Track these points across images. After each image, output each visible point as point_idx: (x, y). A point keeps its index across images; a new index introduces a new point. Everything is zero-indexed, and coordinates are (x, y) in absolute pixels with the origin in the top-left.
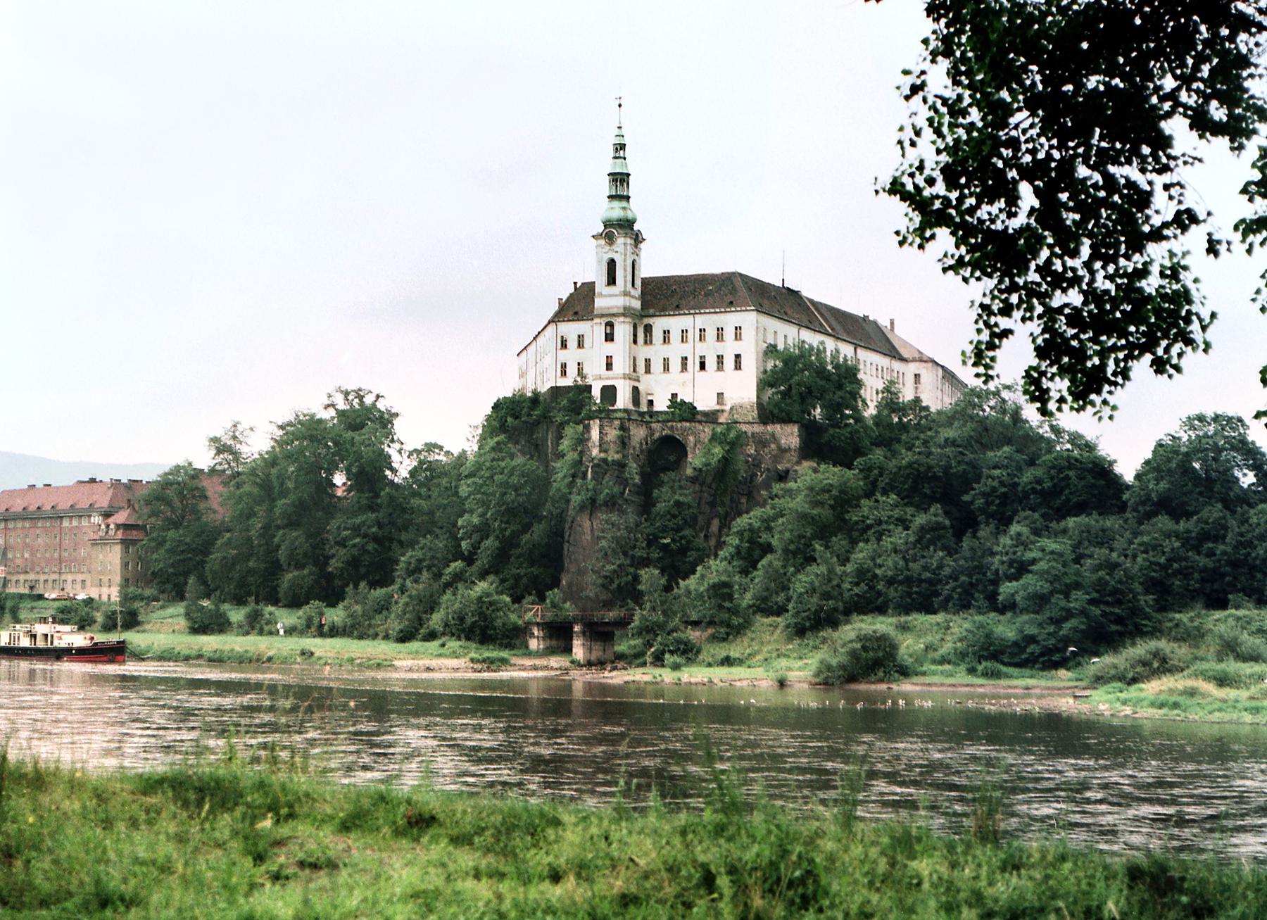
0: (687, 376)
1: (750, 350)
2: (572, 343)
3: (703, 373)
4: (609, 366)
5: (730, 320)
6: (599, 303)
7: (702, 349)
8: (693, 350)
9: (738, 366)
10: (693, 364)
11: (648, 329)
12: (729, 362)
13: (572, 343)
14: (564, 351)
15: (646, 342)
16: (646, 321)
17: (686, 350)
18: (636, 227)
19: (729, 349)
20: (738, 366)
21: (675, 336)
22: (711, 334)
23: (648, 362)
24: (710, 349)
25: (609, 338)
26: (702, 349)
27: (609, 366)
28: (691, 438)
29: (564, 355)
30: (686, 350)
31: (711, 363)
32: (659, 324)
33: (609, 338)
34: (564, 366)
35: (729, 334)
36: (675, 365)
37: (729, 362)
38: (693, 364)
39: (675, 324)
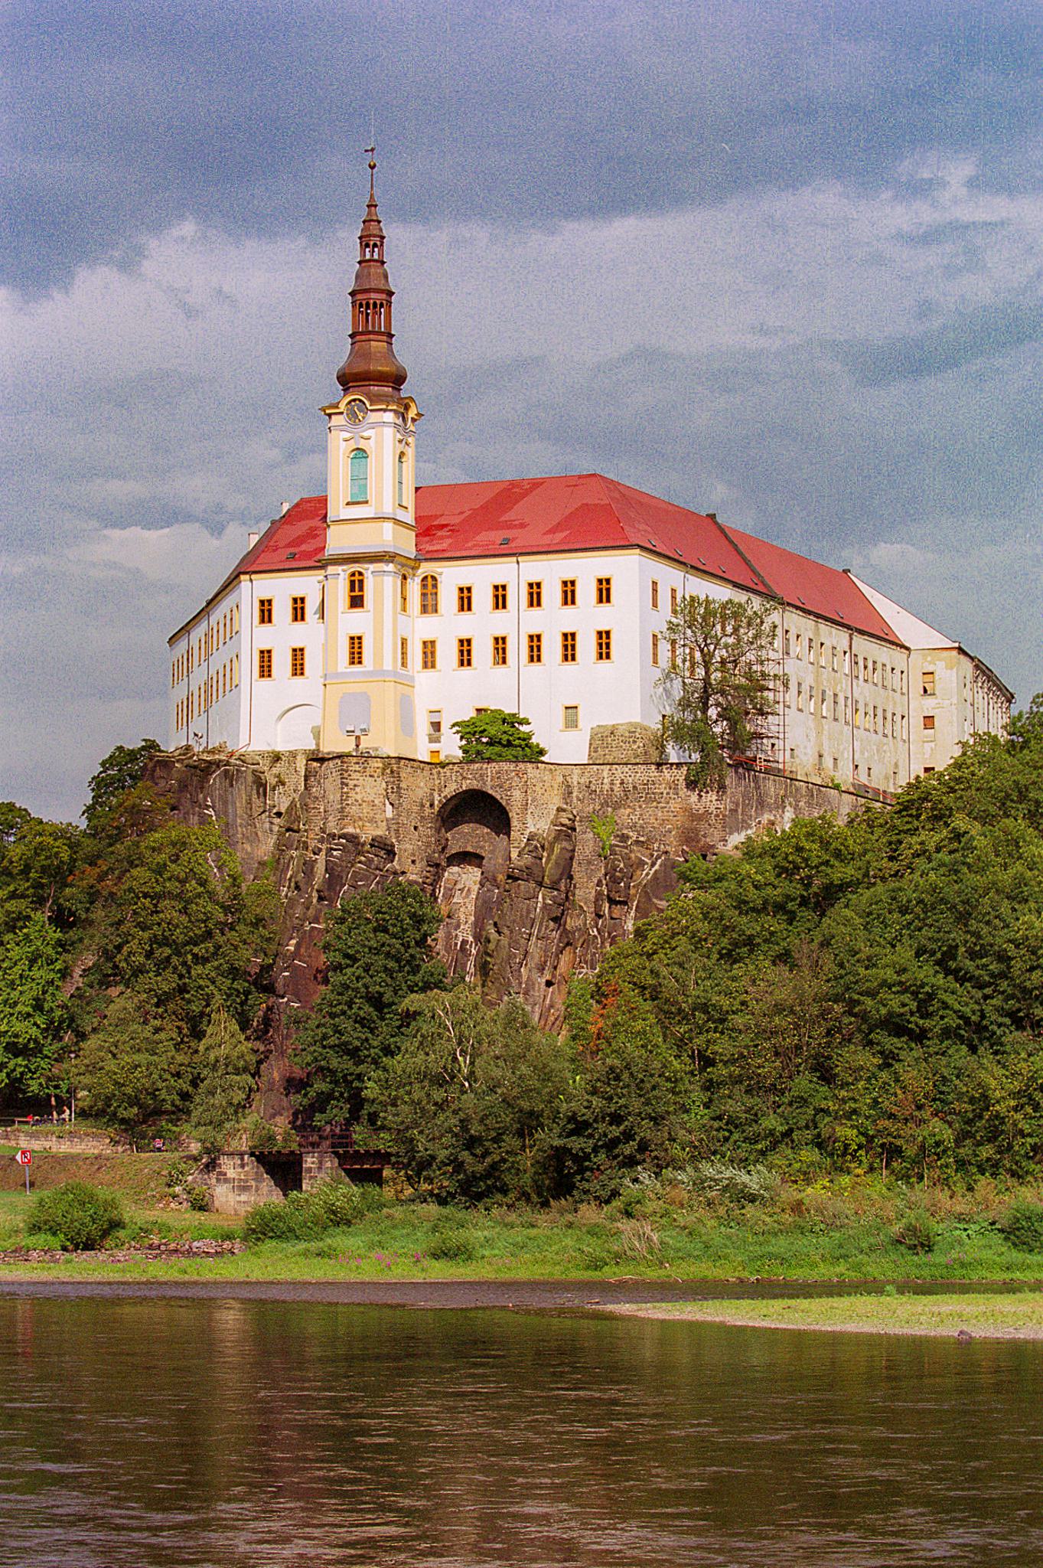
4: (356, 658)
6: (338, 540)
9: (604, 651)
10: (517, 649)
11: (430, 584)
12: (587, 646)
15: (424, 609)
16: (426, 568)
17: (502, 623)
18: (406, 390)
19: (587, 617)
20: (604, 651)
21: (483, 598)
22: (552, 594)
23: (429, 649)
24: (552, 620)
25: (356, 602)
26: (535, 621)
27: (356, 658)
28: (517, 794)
29: (266, 637)
30: (502, 623)
31: (552, 648)
32: (451, 576)
33: (356, 602)
34: (266, 656)
36: (483, 651)
37: (587, 646)
38: (517, 649)
39: (481, 575)
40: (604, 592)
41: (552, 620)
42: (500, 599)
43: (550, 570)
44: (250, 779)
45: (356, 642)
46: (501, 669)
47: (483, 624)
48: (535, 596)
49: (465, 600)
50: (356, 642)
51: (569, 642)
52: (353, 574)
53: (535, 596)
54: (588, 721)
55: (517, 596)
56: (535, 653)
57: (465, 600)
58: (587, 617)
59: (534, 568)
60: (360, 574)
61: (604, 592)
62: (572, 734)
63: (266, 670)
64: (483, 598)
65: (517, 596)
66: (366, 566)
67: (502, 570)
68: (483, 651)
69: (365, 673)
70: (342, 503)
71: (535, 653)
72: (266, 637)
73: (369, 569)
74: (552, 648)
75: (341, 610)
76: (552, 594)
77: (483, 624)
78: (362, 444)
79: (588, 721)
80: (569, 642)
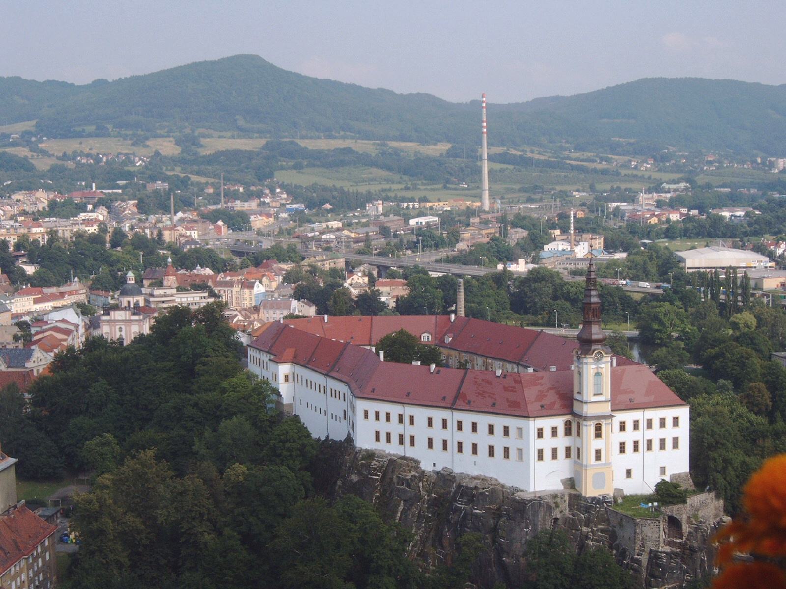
0: (638, 456)
1: (683, 432)
2: (547, 433)
3: (650, 453)
5: (669, 413)
9: (676, 444)
12: (669, 444)
13: (547, 433)
14: (540, 440)
17: (637, 436)
19: (669, 433)
20: (676, 444)
21: (629, 426)
22: (656, 423)
24: (656, 434)
25: (598, 435)
29: (540, 444)
30: (637, 436)
31: (656, 445)
33: (598, 435)
35: (669, 422)
36: (629, 447)
37: (669, 444)
38: (642, 446)
39: (629, 417)
40: (676, 421)
41: (656, 434)
42: (636, 426)
43: (655, 415)
44: (545, 506)
45: (598, 453)
46: (636, 454)
47: (629, 436)
49: (622, 427)
50: (598, 453)
51: (663, 442)
52: (597, 424)
55: (642, 425)
56: (649, 448)
57: (622, 427)
58: (669, 433)
59: (650, 414)
60: (600, 424)
61: (676, 421)
65: (642, 425)
66: (602, 421)
67: (637, 415)
68: (629, 447)
69: (602, 464)
71: (649, 448)
72: (540, 444)
73: (604, 422)
74: (656, 445)
75: (592, 439)
76: (656, 423)
77: (629, 436)
78: (600, 370)
80: (663, 442)
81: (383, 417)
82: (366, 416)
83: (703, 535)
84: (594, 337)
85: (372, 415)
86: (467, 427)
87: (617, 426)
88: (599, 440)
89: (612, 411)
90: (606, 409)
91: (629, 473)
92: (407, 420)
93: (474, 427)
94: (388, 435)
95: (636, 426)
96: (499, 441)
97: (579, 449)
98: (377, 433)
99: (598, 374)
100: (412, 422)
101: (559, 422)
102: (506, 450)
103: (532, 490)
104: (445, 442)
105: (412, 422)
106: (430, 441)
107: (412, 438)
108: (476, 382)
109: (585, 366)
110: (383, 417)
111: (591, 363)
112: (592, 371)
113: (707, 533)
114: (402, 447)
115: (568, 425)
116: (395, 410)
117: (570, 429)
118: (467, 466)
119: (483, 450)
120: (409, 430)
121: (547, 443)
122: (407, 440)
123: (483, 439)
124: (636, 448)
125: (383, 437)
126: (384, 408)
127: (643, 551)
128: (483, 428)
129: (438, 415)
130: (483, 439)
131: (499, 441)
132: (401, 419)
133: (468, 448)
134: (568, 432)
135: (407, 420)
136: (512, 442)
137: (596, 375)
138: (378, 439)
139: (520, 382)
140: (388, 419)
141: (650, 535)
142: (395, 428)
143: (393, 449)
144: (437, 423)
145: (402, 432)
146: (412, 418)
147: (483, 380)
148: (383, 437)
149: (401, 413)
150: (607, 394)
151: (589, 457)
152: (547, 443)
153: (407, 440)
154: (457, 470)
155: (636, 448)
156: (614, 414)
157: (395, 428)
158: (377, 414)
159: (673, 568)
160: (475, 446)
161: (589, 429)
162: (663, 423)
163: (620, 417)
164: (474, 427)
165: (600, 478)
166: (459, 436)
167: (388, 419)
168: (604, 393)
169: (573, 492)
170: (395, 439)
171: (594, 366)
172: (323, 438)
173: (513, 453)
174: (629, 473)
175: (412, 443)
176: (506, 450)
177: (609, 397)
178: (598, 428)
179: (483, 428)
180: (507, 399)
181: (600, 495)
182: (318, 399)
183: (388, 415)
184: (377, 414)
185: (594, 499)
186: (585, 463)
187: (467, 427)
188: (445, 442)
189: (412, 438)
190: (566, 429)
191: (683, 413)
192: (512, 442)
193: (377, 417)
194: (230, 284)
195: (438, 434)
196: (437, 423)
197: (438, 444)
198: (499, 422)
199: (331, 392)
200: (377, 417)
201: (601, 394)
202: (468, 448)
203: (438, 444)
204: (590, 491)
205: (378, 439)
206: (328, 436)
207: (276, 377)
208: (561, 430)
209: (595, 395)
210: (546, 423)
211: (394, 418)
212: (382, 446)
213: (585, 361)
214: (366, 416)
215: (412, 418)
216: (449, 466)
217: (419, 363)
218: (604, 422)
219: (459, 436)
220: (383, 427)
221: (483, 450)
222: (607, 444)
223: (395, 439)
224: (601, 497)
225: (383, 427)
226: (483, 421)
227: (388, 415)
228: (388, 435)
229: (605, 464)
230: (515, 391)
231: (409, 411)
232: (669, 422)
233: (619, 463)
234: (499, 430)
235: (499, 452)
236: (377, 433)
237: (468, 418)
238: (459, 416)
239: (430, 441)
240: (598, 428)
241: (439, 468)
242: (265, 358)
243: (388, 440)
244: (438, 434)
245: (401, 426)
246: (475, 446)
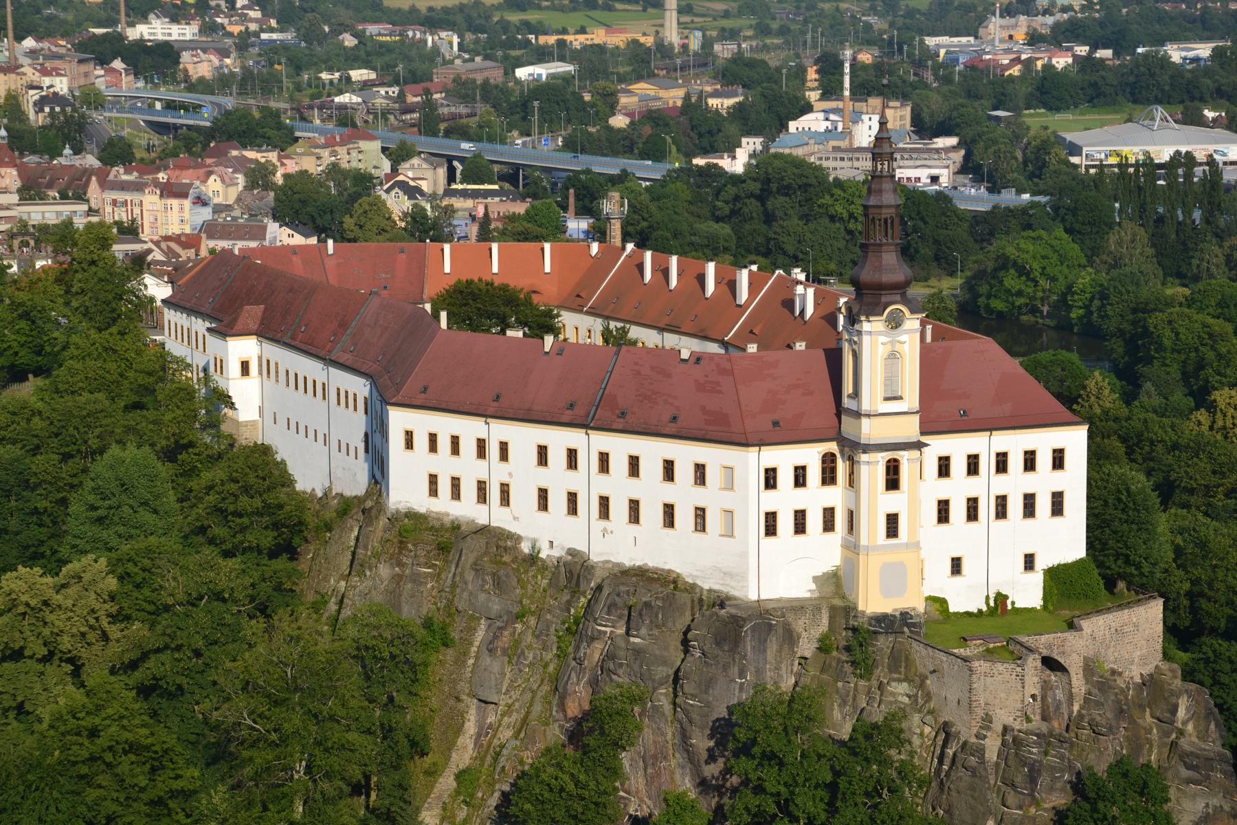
0: (978, 527)
1: (1074, 480)
2: (785, 478)
4: (892, 531)
5: (1044, 441)
7: (1001, 484)
8: (986, 486)
10: (986, 509)
12: (1043, 505)
13: (785, 478)
19: (1044, 482)
21: (959, 466)
22: (1016, 462)
24: (1015, 484)
25: (893, 483)
26: (1001, 484)
27: (892, 531)
29: (771, 500)
31: (1015, 506)
33: (893, 483)
35: (1044, 460)
36: (958, 511)
37: (1043, 505)
38: (986, 509)
39: (958, 446)
40: (1058, 460)
41: (1015, 484)
42: (973, 466)
43: (1014, 442)
44: (780, 631)
45: (892, 520)
46: (973, 525)
47: (959, 488)
48: (1002, 464)
49: (944, 468)
50: (892, 520)
53: (1002, 464)
54: (1041, 564)
55: (987, 464)
56: (1001, 512)
57: (944, 468)
58: (1044, 482)
60: (896, 460)
61: (1058, 460)
62: (1030, 575)
63: (771, 528)
64: (959, 466)
65: (987, 464)
68: (958, 511)
70: (880, 395)
71: (1001, 512)
72: (771, 500)
73: (904, 457)
74: (1015, 506)
76: (1016, 462)
77: (959, 488)
78: (898, 347)
79: (1041, 564)
81: (444, 444)
82: (409, 444)
83: (1119, 702)
84: (887, 278)
85: (421, 442)
86: (619, 465)
87: (932, 467)
88: (893, 494)
89: (922, 433)
90: (909, 428)
91: (956, 566)
92: (494, 451)
93: (634, 465)
94: (456, 483)
95: (973, 466)
96: (684, 494)
97: (851, 514)
98: (433, 479)
99: (893, 356)
100: (504, 456)
101: (810, 455)
102: (700, 513)
103: (753, 597)
104: (572, 498)
105: (504, 456)
106: (543, 494)
107: (505, 490)
108: (639, 373)
109: (866, 338)
110: (444, 444)
111: (879, 333)
112: (881, 348)
113: (1126, 698)
114: (484, 508)
115: (828, 464)
116: (470, 428)
117: (833, 470)
118: (618, 546)
119: (652, 514)
120: (497, 473)
121: (785, 500)
122: (494, 494)
123: (651, 490)
124: (972, 515)
125: (444, 487)
126: (446, 424)
127: (988, 728)
128: (651, 468)
129: (559, 439)
130: (651, 490)
131: (684, 494)
132: (481, 447)
133: (619, 510)
134: (829, 477)
135: (494, 451)
136: (711, 497)
137: (890, 355)
138: (433, 492)
139: (731, 373)
140: (455, 449)
141: (1003, 695)
142: (469, 468)
143: (467, 510)
144: (557, 457)
145: (484, 477)
146: (504, 447)
147: (653, 368)
148: (444, 487)
149: (483, 436)
150: (911, 398)
151: (872, 529)
152: (785, 500)
153: (494, 494)
154: (597, 555)
155: (972, 515)
156: (924, 439)
157: (469, 468)
158: (433, 438)
159: (1052, 769)
160: (634, 506)
161: (873, 469)
162: (1030, 462)
163: (939, 445)
164: (634, 465)
165: (894, 577)
166: (602, 485)
167: (455, 449)
168: (906, 396)
169: (837, 602)
170: (469, 490)
171: (883, 339)
172: (320, 494)
173: (712, 519)
174: (956, 566)
175: (505, 499)
176: (700, 513)
177: (916, 405)
178: (893, 469)
179: (651, 468)
180: (703, 408)
181: (895, 610)
182: (311, 410)
183: (455, 441)
184: (433, 438)
185: (882, 619)
186: (864, 541)
187: (619, 465)
188: (572, 498)
189: (505, 490)
190: (824, 471)
191: (1075, 440)
192: (711, 497)
193: (433, 447)
194: (138, 187)
195: (558, 479)
196: (557, 457)
197: (558, 501)
198: (686, 454)
199: (338, 394)
200: (433, 447)
201: (901, 398)
202: (619, 510)
203: (558, 501)
204: (874, 600)
205: (433, 492)
206: (330, 489)
207: (221, 365)
208: (814, 474)
209: (887, 399)
210: (785, 458)
211: (468, 447)
212: (443, 506)
213: (866, 326)
214: (409, 444)
215: (504, 447)
216: (581, 546)
217: (520, 334)
218: (904, 457)
219: (602, 485)
220: (444, 465)
221: (652, 514)
222: (914, 503)
223: (469, 490)
224: (897, 614)
225: (444, 465)
226: (653, 450)
227: (455, 441)
228: (456, 483)
229: (907, 545)
230: (720, 392)
231: (500, 430)
232: (1044, 460)
233: (936, 543)
234: (684, 472)
235: (684, 517)
236: (433, 479)
237: (620, 446)
238: (603, 441)
239: (543, 494)
240: (893, 469)
241: (556, 553)
242: (200, 326)
243: (456, 494)
244: (558, 479)
245: (483, 464)
246: (634, 506)
